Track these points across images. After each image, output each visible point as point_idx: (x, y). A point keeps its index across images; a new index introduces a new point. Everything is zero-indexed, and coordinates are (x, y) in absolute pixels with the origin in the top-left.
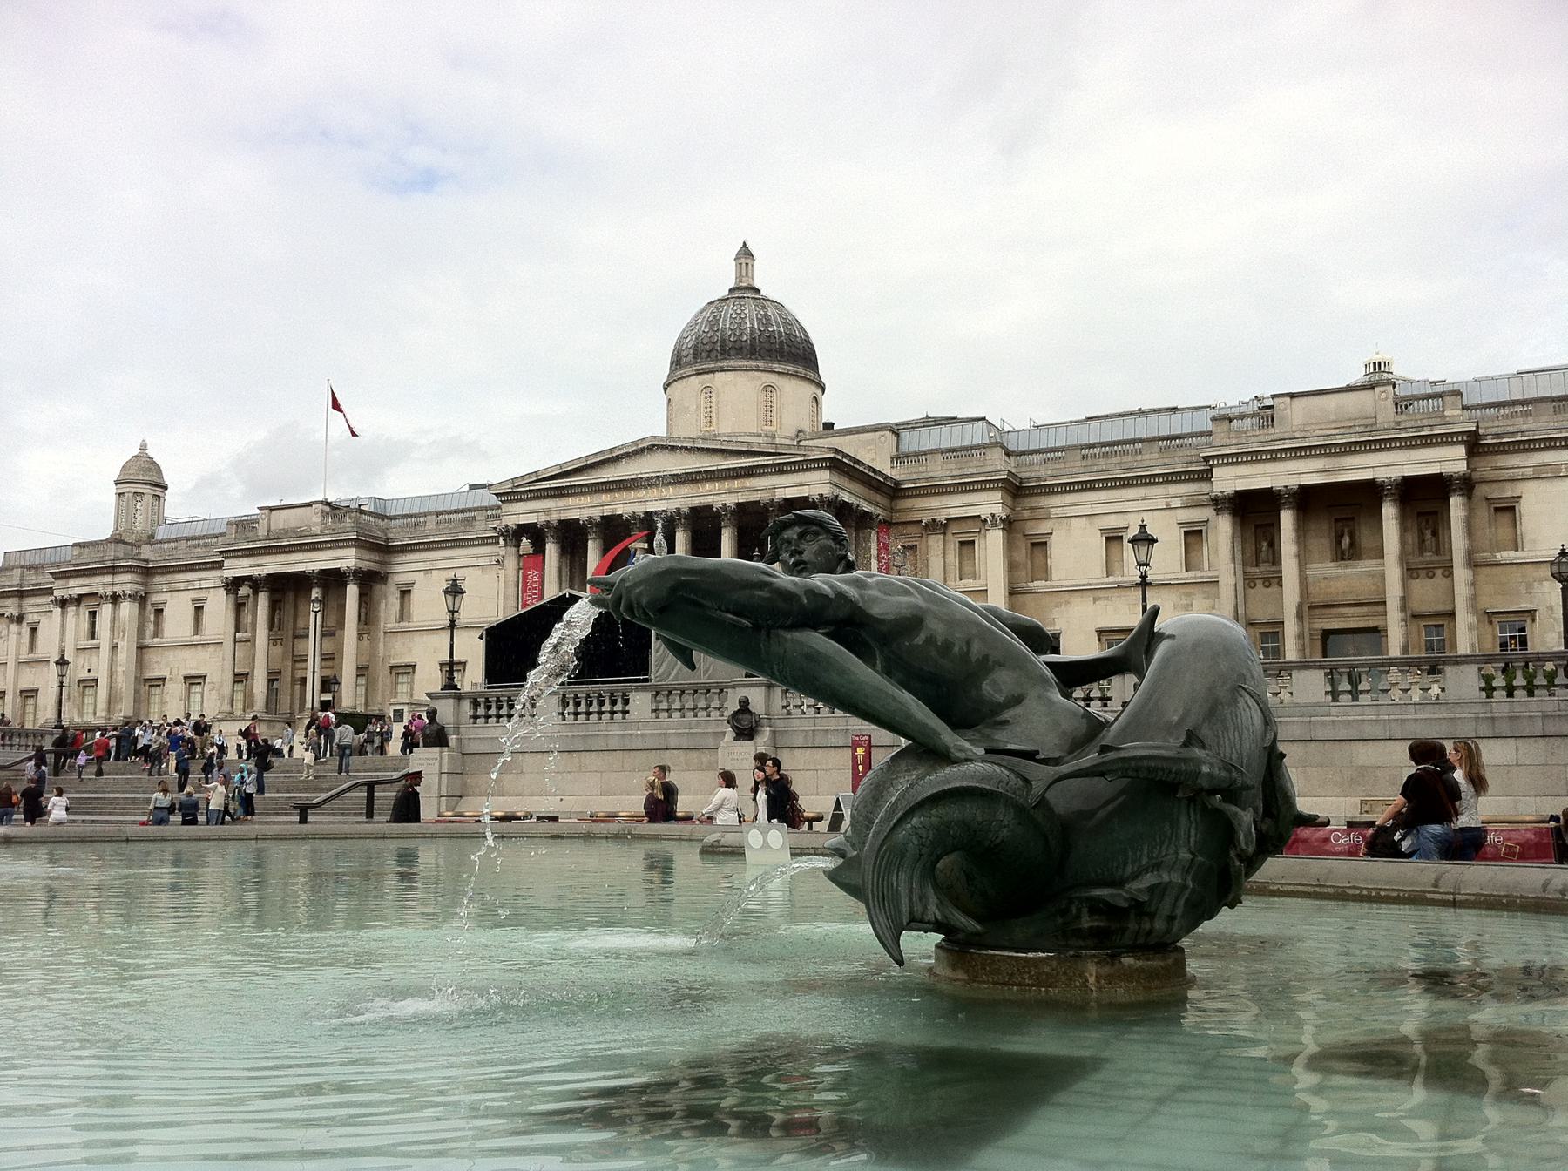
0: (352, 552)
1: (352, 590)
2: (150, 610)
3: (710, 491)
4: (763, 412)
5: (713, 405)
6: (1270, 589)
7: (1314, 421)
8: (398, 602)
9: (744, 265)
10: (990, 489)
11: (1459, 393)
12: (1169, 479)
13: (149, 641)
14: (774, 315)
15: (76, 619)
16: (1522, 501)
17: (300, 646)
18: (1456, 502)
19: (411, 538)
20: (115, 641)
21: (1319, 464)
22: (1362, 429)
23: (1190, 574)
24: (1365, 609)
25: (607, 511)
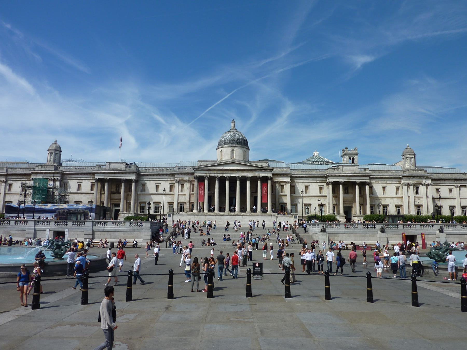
0: (135, 175)
1: (133, 184)
2: (62, 183)
9: (234, 124)
10: (288, 176)
12: (317, 177)
14: (236, 135)
17: (116, 196)
18: (367, 187)
19: (146, 173)
21: (347, 178)
22: (354, 173)
23: (320, 195)
25: (221, 175)
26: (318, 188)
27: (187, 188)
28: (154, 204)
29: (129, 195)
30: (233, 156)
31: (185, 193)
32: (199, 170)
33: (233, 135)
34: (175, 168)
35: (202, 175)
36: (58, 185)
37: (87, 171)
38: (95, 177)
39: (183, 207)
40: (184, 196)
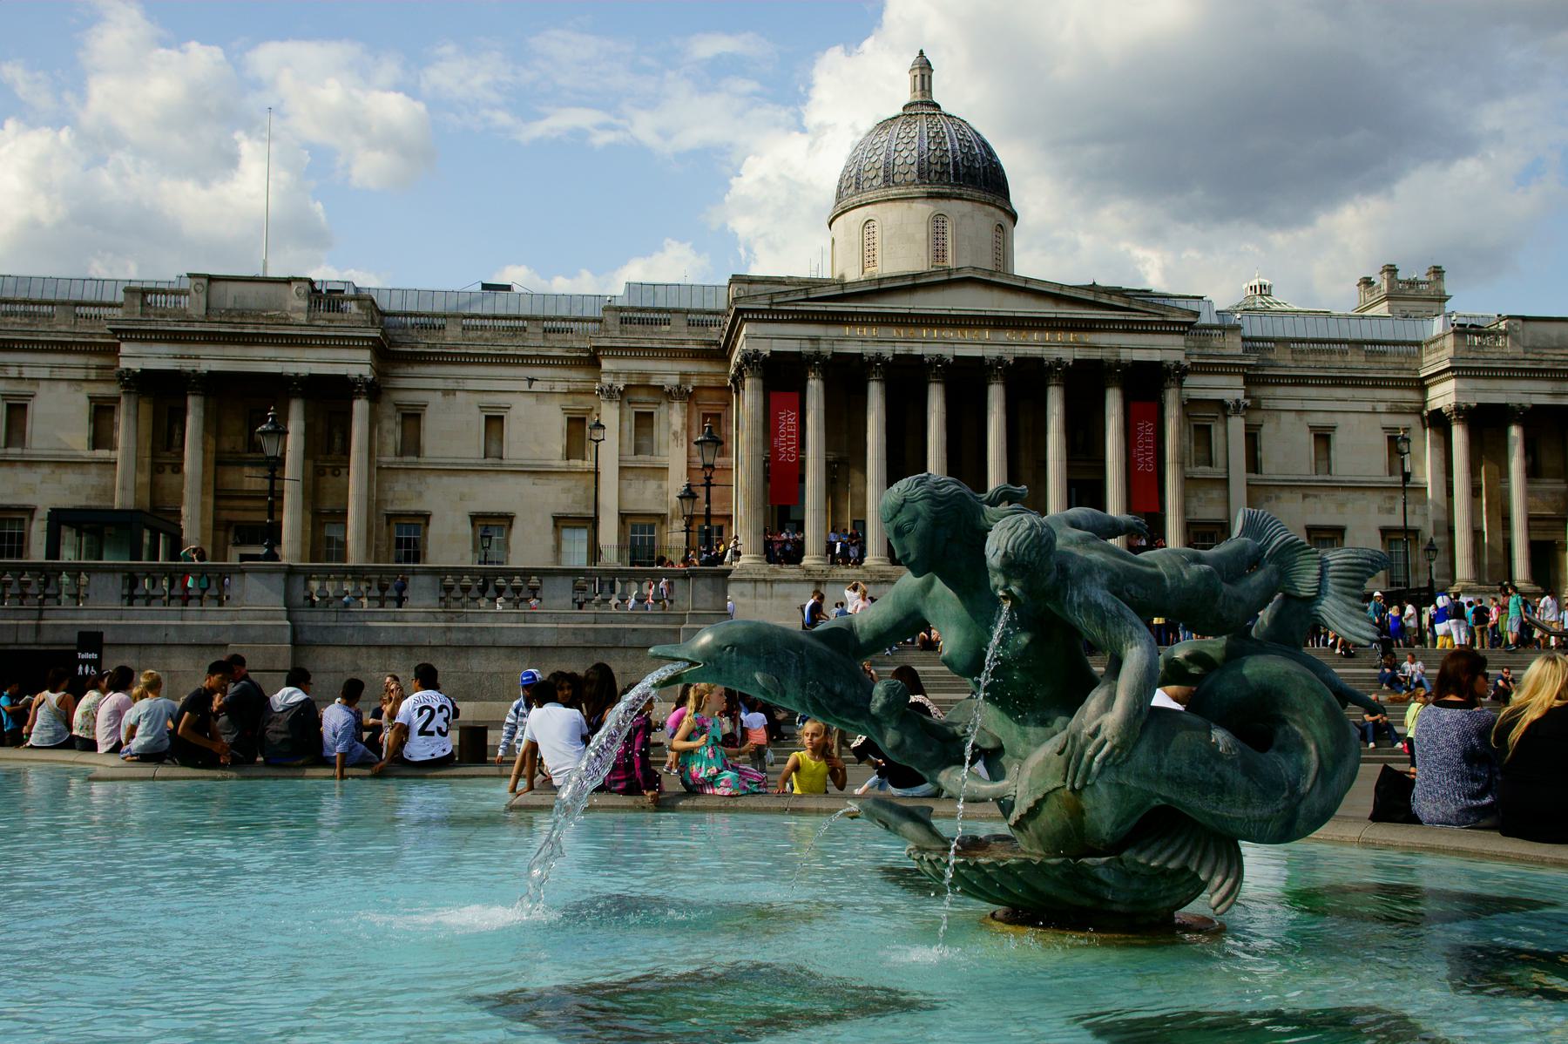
1: (360, 407)
3: (1038, 341)
7: (1539, 344)
10: (1235, 374)
12: (1377, 383)
24: (1543, 524)
25: (901, 349)
26: (1381, 441)
27: (675, 434)
28: (473, 525)
29: (328, 470)
30: (939, 253)
31: (658, 461)
32: (772, 315)
34: (600, 321)
35: (793, 347)
37: (64, 328)
38: (124, 364)
39: (652, 540)
40: (654, 479)
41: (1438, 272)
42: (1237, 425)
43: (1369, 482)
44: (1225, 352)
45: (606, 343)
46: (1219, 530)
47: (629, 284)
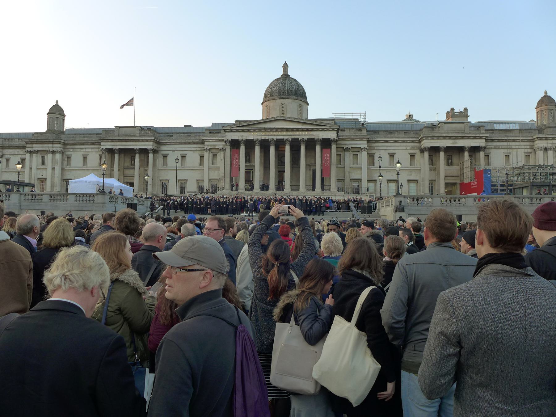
0: (151, 143)
1: (151, 155)
2: (65, 156)
3: (298, 134)
4: (298, 112)
5: (285, 108)
6: (432, 172)
8: (163, 160)
11: (483, 126)
12: (407, 141)
13: (64, 167)
15: (36, 159)
16: (491, 154)
17: (128, 172)
18: (482, 154)
20: (53, 166)
23: (412, 167)
24: (454, 178)
25: (263, 138)
26: (408, 157)
27: (222, 159)
30: (283, 113)
33: (284, 82)
36: (58, 159)
38: (102, 147)
41: (466, 109)
42: (365, 154)
43: (406, 168)
44: (361, 135)
45: (205, 138)
46: (359, 181)
47: (212, 124)
